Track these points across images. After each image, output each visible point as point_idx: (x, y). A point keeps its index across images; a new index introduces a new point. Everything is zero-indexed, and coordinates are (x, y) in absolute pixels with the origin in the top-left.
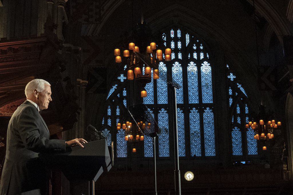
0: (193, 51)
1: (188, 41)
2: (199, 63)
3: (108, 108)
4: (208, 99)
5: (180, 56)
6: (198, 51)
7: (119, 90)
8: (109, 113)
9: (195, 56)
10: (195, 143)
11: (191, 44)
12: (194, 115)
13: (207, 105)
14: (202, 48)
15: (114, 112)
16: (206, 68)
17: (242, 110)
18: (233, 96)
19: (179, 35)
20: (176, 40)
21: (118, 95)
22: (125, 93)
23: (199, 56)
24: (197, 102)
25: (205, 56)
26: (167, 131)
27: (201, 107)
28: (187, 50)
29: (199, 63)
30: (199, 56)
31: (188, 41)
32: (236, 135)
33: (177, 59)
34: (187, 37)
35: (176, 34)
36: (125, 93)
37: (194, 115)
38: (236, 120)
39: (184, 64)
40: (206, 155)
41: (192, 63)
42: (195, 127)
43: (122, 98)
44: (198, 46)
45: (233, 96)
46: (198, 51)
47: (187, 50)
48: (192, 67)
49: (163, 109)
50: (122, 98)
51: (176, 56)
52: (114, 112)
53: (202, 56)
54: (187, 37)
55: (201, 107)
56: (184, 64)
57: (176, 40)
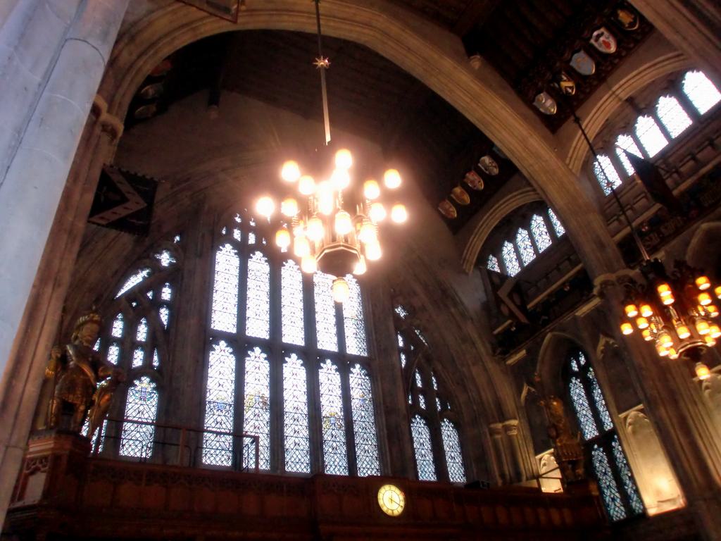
3: (114, 318)
4: (355, 346)
7: (153, 285)
8: (118, 329)
10: (333, 437)
13: (355, 360)
15: (130, 329)
17: (427, 382)
18: (405, 350)
21: (150, 295)
22: (166, 294)
24: (334, 348)
26: (265, 403)
27: (343, 362)
32: (420, 432)
36: (166, 294)
37: (329, 375)
38: (416, 401)
40: (360, 474)
42: (331, 405)
43: (158, 303)
45: (405, 350)
49: (257, 350)
50: (158, 303)
52: (130, 329)
55: (343, 362)
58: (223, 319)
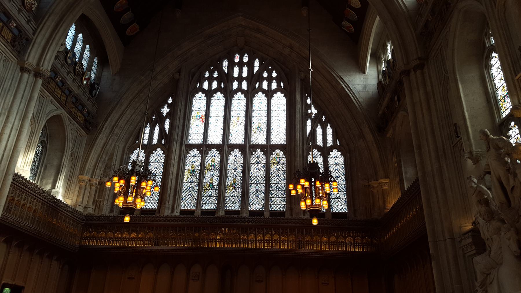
0: (260, 79)
1: (256, 69)
2: (269, 94)
5: (244, 86)
6: (270, 79)
9: (265, 85)
11: (261, 72)
12: (258, 159)
14: (274, 75)
16: (279, 101)
19: (246, 59)
20: (241, 64)
23: (269, 86)
25: (278, 85)
28: (254, 79)
29: (269, 94)
30: (269, 86)
31: (256, 69)
33: (240, 89)
34: (257, 63)
35: (241, 58)
37: (258, 159)
39: (249, 95)
41: (260, 93)
44: (270, 73)
46: (270, 79)
47: (254, 79)
48: (260, 100)
51: (240, 85)
53: (274, 85)
54: (257, 63)
55: (268, 149)
56: (249, 95)
57: (241, 64)
58: (195, 136)
